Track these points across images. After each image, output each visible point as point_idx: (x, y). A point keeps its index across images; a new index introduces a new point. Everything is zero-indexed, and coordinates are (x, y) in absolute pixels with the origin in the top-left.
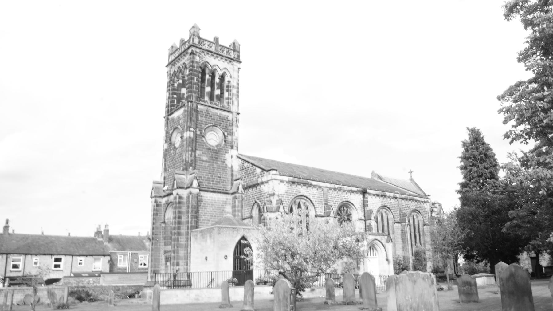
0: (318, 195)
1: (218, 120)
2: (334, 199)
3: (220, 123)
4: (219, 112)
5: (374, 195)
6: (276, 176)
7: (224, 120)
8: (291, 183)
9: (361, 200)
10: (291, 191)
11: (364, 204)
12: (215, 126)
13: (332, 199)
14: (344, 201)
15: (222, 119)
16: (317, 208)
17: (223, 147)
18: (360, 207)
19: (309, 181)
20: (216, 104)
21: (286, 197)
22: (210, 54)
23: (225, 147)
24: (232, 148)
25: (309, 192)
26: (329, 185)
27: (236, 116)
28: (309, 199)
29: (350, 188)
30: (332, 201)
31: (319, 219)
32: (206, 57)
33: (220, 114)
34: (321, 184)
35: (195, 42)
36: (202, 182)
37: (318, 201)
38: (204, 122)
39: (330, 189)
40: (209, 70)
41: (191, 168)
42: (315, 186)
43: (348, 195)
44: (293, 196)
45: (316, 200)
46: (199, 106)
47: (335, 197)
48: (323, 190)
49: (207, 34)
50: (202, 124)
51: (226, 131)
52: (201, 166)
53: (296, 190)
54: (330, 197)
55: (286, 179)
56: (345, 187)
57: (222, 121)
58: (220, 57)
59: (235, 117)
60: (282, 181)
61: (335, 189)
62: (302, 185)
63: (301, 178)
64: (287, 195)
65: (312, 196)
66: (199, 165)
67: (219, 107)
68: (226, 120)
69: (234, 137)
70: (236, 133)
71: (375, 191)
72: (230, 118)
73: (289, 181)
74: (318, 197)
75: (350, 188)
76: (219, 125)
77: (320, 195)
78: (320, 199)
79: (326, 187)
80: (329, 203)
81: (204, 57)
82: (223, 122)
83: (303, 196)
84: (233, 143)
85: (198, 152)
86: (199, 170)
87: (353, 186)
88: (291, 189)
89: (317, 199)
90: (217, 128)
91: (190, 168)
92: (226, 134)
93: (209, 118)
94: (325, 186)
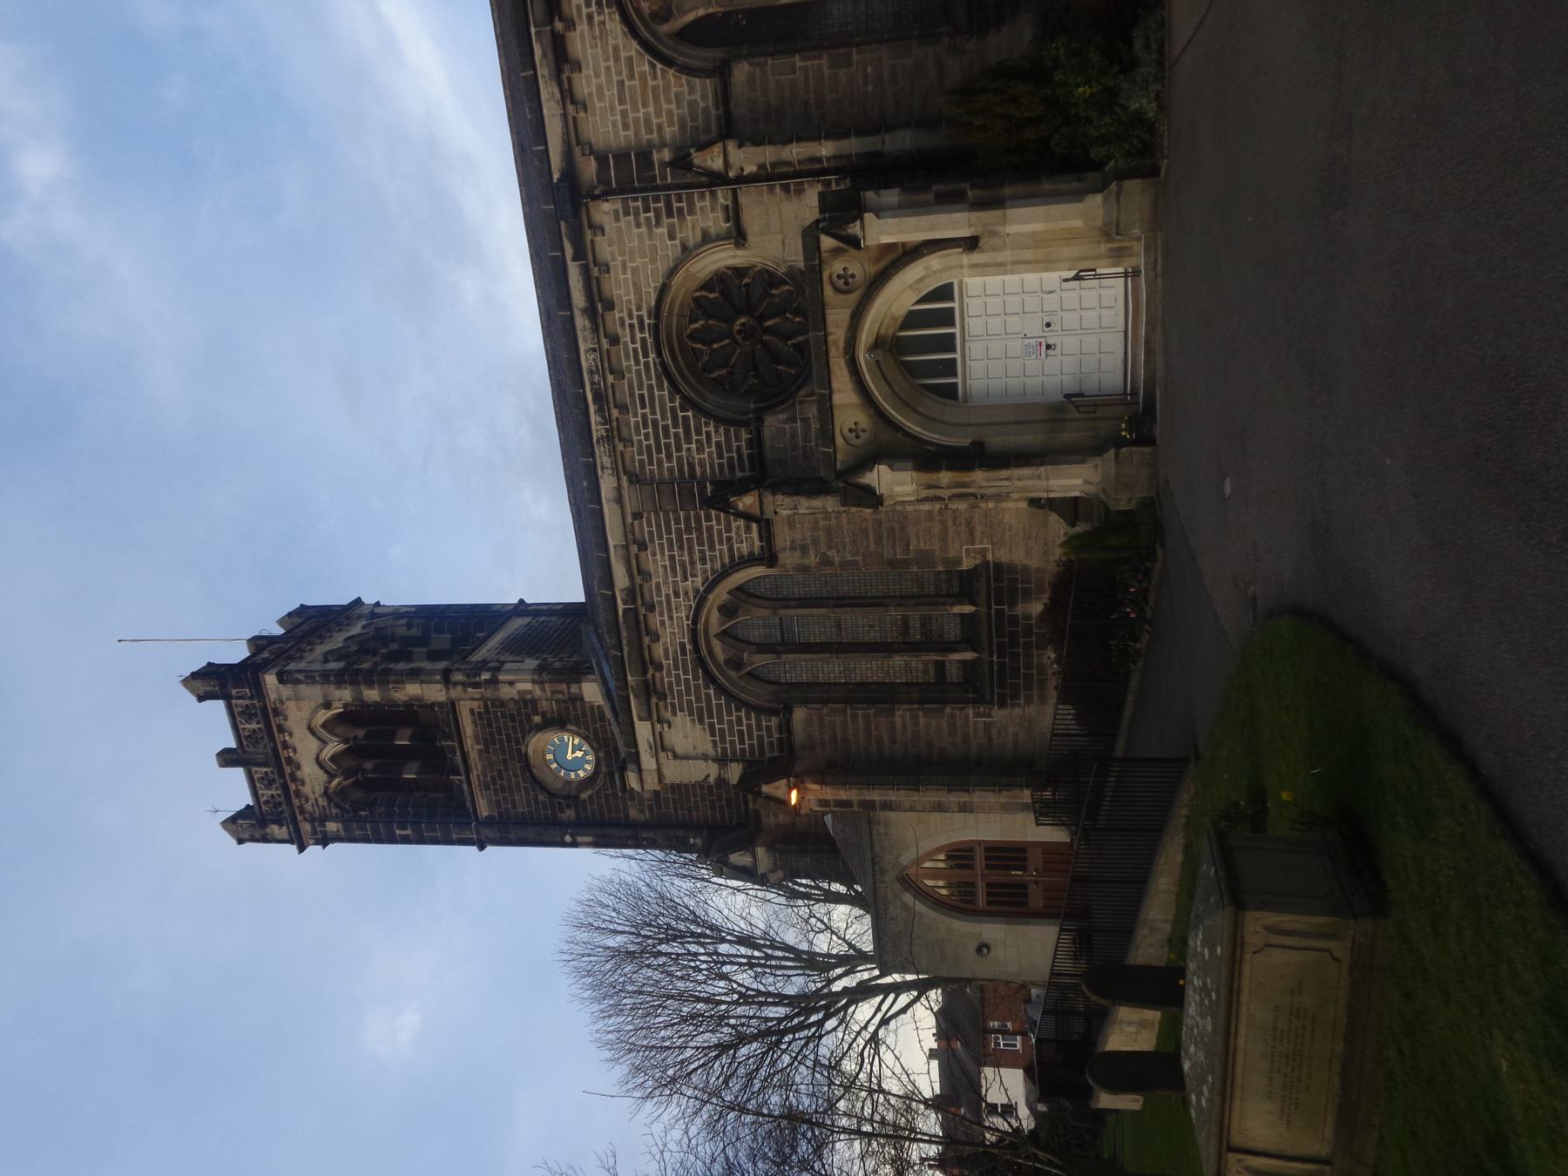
0: (670, 541)
1: (502, 749)
2: (665, 428)
3: (509, 741)
4: (473, 748)
5: (568, 95)
6: (643, 773)
7: (490, 726)
8: (654, 700)
9: (627, 213)
10: (688, 694)
11: (644, 190)
12: (524, 759)
13: (668, 446)
14: (663, 364)
15: (492, 733)
16: (731, 549)
17: (587, 729)
18: (665, 220)
19: (621, 607)
20: (454, 753)
21: (721, 721)
22: (292, 787)
23: (585, 723)
24: (581, 699)
25: (668, 596)
26: (607, 484)
27: (459, 688)
28: (702, 600)
29: (581, 322)
30: (679, 449)
31: (783, 536)
32: (311, 796)
33: (480, 744)
34: (614, 538)
35: (286, 837)
36: (729, 800)
37: (701, 544)
38: (527, 794)
39: (621, 468)
40: (345, 779)
41: (692, 841)
42: (638, 572)
43: (622, 324)
44: (707, 687)
45: (697, 556)
46: (484, 811)
47: (655, 422)
48: (637, 516)
49: (235, 790)
50: (537, 801)
51: (529, 718)
52: (675, 803)
53: (676, 668)
54: (660, 463)
55: (643, 731)
56: (584, 364)
57: (499, 733)
58: (283, 754)
59: (465, 691)
60: (660, 746)
61: (615, 435)
62: (646, 640)
63: (622, 654)
64: (710, 716)
65: (685, 579)
66: (675, 809)
67: (457, 746)
68: (489, 720)
69: (538, 692)
70: (521, 686)
71: (544, 94)
72: (475, 705)
73: (649, 717)
74: (680, 540)
75: (581, 322)
76: (518, 743)
77: (669, 532)
78: (689, 530)
79: (619, 500)
80: (691, 466)
81: (316, 800)
82: (499, 729)
83: (694, 634)
84: (561, 696)
85: (633, 813)
86: (690, 809)
87: (565, 300)
88: (680, 692)
89: (690, 549)
90: (530, 752)
91: (695, 844)
92: (537, 719)
93: (510, 781)
94: (616, 507)
